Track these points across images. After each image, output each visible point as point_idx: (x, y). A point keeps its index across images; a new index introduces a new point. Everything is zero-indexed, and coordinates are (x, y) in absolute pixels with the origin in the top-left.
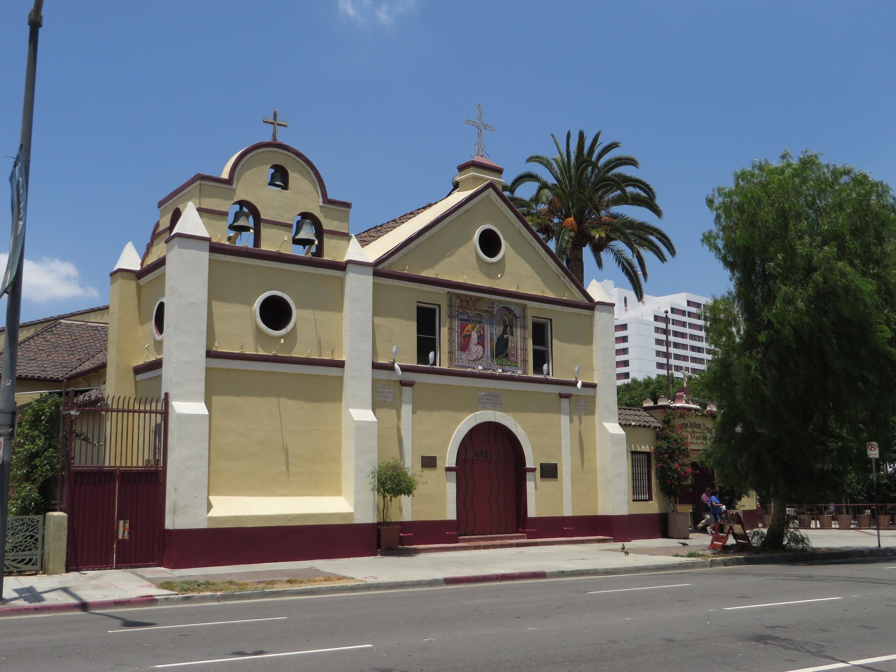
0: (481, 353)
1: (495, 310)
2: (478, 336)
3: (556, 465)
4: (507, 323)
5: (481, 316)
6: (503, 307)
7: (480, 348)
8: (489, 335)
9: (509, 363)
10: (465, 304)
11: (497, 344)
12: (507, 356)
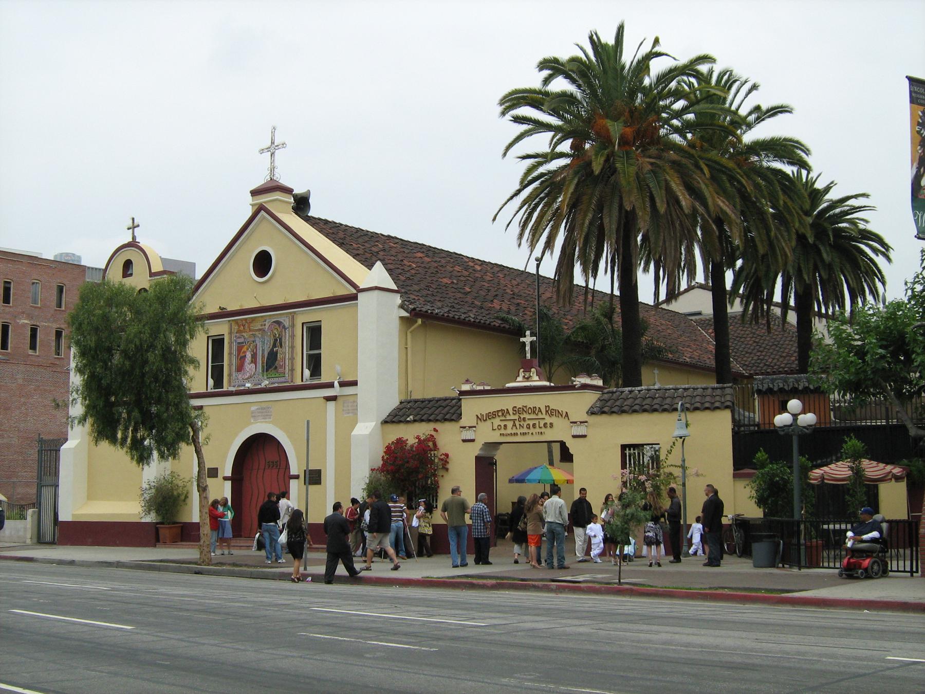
0: (254, 370)
1: (267, 327)
2: (252, 355)
3: (320, 471)
4: (277, 336)
5: (254, 336)
6: (274, 322)
7: (253, 365)
8: (261, 352)
9: (277, 375)
10: (242, 328)
11: (268, 358)
12: (276, 368)
